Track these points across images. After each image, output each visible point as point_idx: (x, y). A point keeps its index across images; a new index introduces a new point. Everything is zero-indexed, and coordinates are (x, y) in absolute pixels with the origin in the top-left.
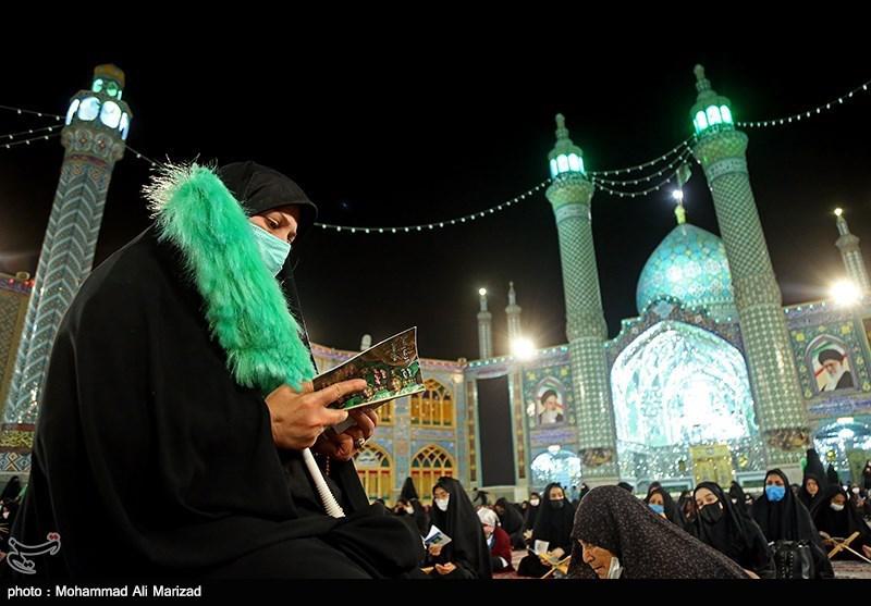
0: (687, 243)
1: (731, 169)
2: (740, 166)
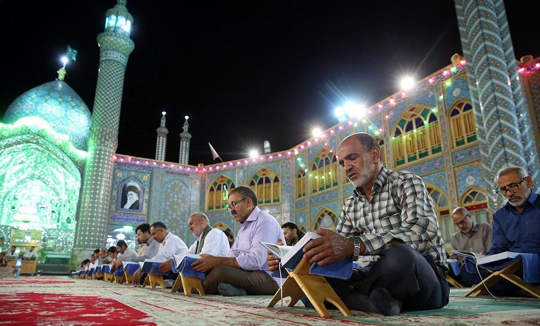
0: (62, 94)
1: (117, 59)
2: (124, 61)
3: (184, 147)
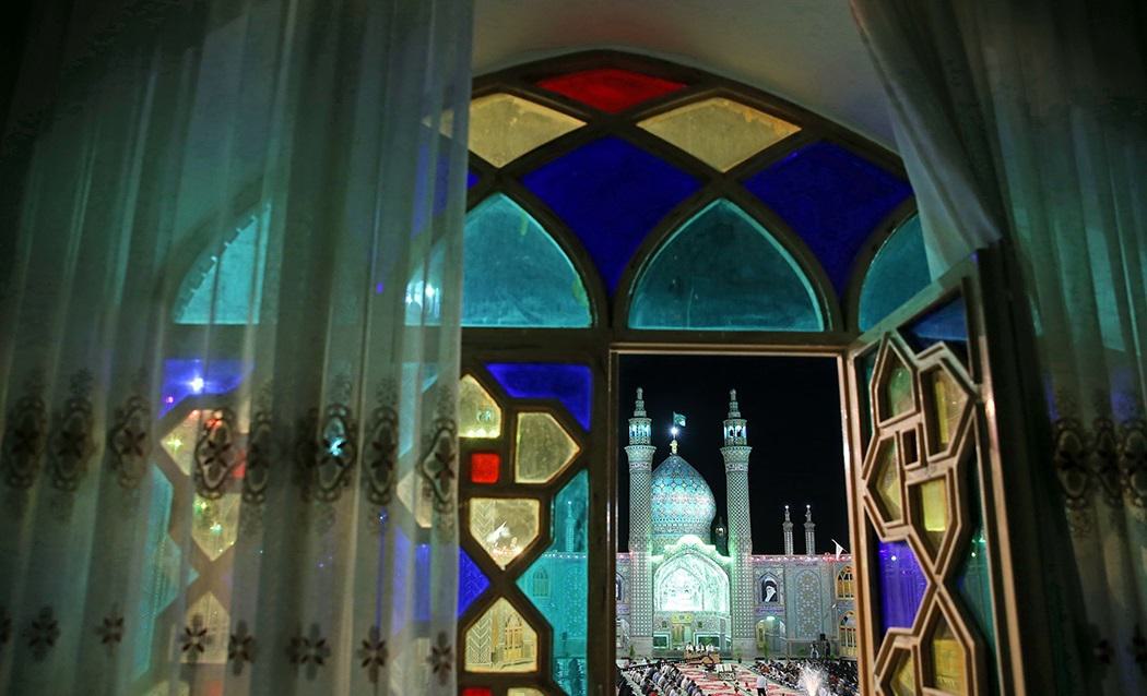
3: (810, 538)
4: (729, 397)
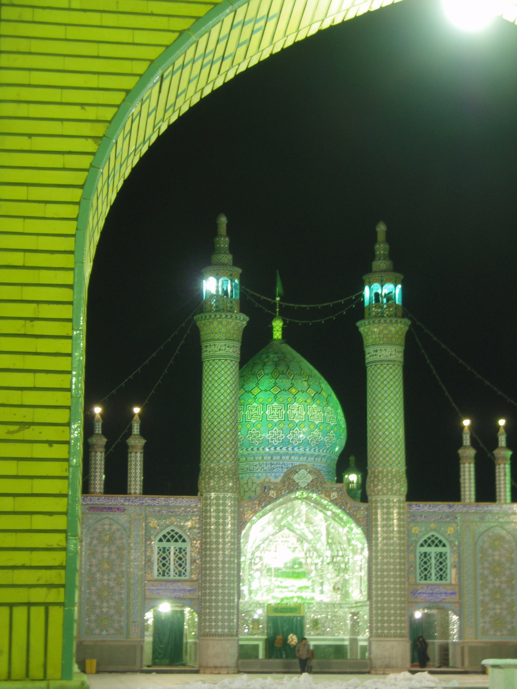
4: (375, 235)
